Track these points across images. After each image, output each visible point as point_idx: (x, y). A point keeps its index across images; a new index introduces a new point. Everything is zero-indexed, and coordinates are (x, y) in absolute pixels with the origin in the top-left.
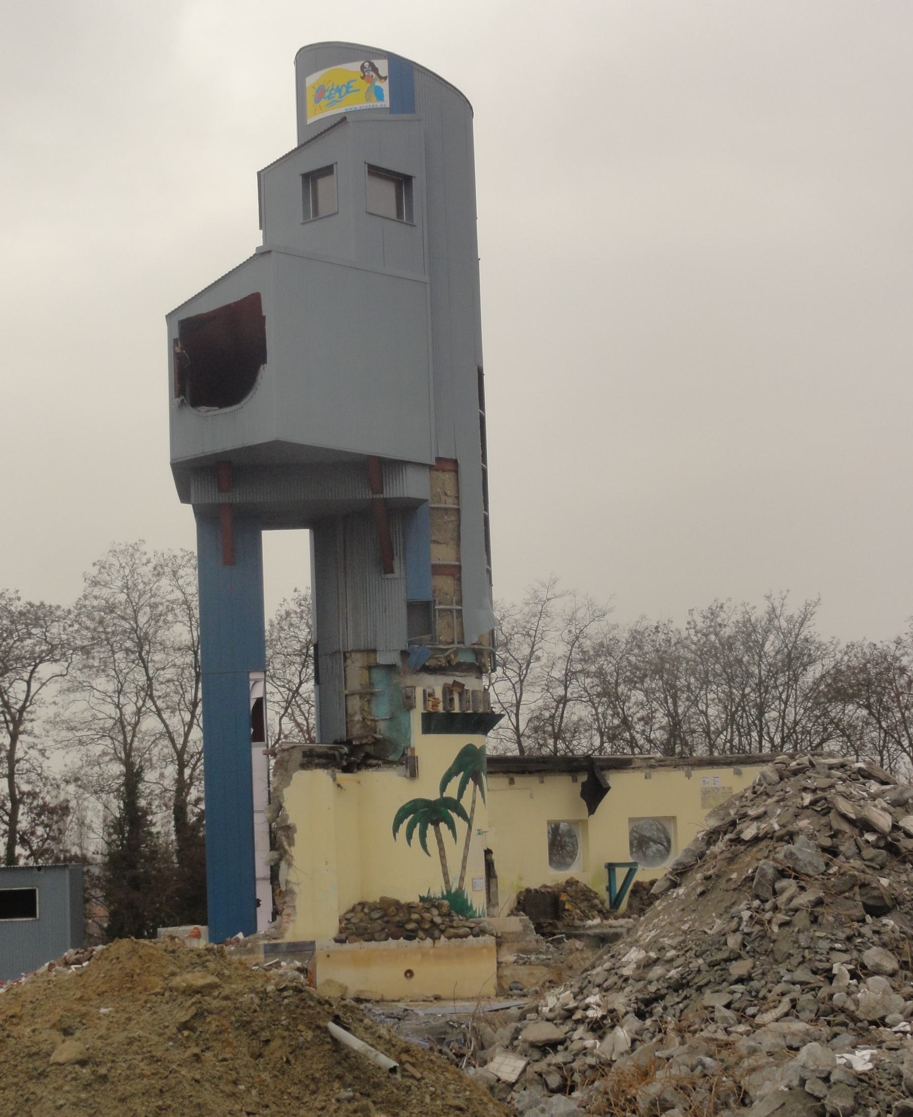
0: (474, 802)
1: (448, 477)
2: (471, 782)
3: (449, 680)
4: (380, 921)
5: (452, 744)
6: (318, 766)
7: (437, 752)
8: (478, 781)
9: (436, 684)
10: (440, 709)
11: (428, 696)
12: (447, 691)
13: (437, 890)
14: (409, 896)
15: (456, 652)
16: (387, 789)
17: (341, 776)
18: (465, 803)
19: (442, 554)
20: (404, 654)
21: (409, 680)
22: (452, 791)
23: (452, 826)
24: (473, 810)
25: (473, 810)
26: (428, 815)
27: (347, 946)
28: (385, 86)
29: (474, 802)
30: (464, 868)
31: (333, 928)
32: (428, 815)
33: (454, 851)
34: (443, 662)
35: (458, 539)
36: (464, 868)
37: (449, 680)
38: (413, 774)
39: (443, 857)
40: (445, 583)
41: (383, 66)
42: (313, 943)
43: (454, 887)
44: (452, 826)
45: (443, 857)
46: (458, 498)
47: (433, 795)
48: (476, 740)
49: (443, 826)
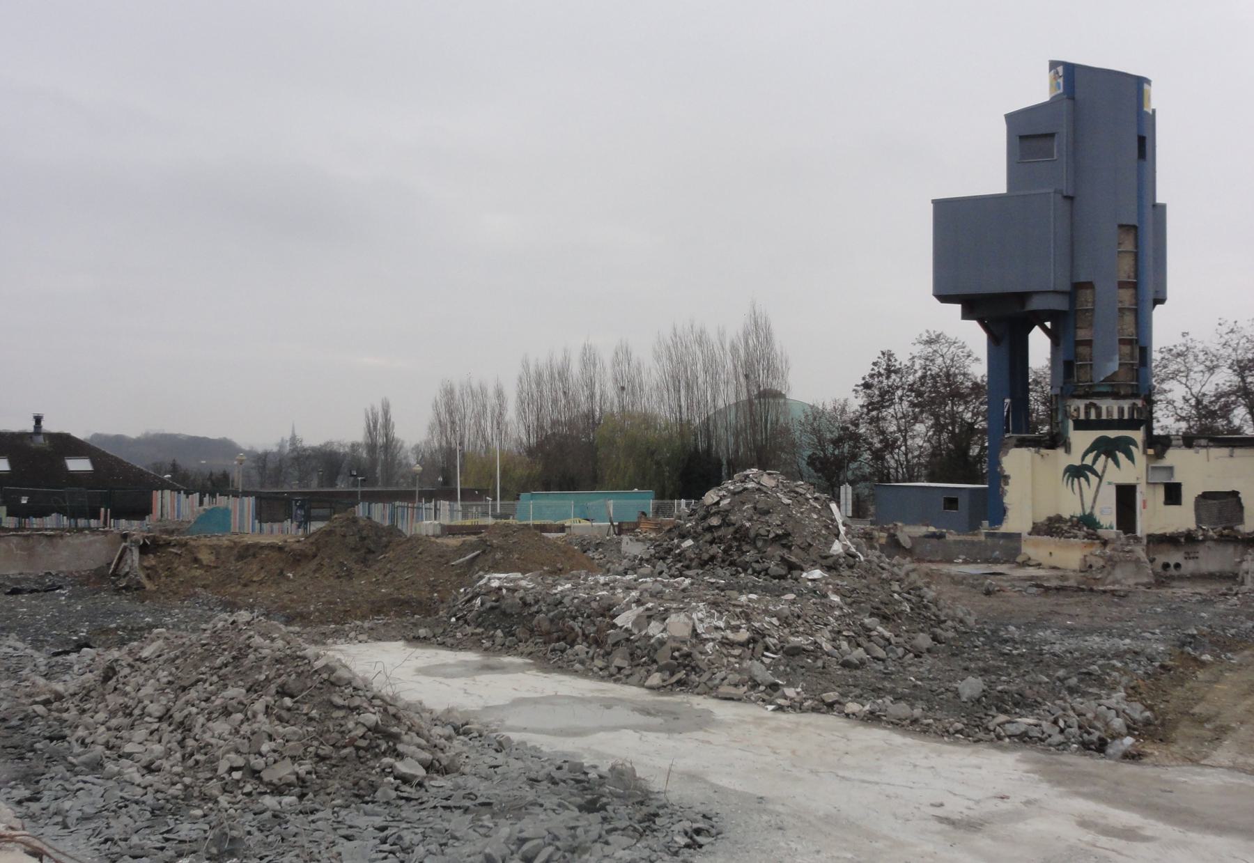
0: (1105, 467)
1: (1088, 291)
2: (1103, 457)
3: (1088, 402)
4: (1052, 527)
5: (1092, 436)
6: (1027, 446)
7: (1081, 440)
8: (1111, 454)
9: (1081, 404)
10: (1082, 417)
11: (1077, 410)
12: (1087, 407)
13: (1078, 513)
14: (1066, 516)
15: (1090, 386)
16: (1062, 459)
17: (1043, 451)
18: (1098, 467)
19: (1082, 334)
20: (1062, 388)
21: (1069, 402)
22: (1089, 460)
23: (1087, 479)
24: (1103, 472)
25: (1103, 472)
26: (1076, 472)
27: (1033, 537)
28: (1061, 81)
29: (1105, 467)
30: (1094, 501)
31: (1029, 527)
32: (1076, 472)
33: (1089, 493)
34: (1082, 393)
35: (1091, 325)
36: (1094, 501)
37: (1088, 402)
38: (1068, 450)
39: (1081, 496)
40: (1082, 350)
41: (1060, 69)
42: (1019, 535)
43: (1088, 511)
44: (1087, 479)
45: (1081, 496)
46: (1094, 302)
47: (1077, 463)
48: (1112, 434)
49: (1082, 479)
